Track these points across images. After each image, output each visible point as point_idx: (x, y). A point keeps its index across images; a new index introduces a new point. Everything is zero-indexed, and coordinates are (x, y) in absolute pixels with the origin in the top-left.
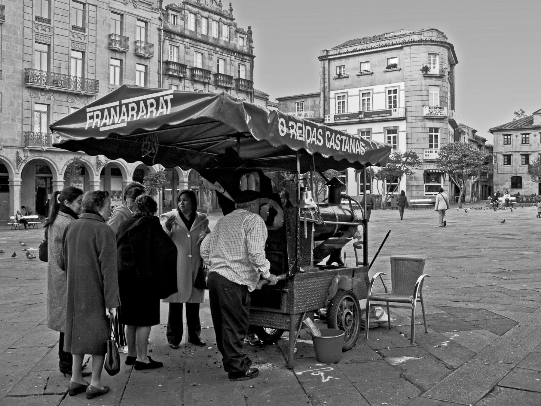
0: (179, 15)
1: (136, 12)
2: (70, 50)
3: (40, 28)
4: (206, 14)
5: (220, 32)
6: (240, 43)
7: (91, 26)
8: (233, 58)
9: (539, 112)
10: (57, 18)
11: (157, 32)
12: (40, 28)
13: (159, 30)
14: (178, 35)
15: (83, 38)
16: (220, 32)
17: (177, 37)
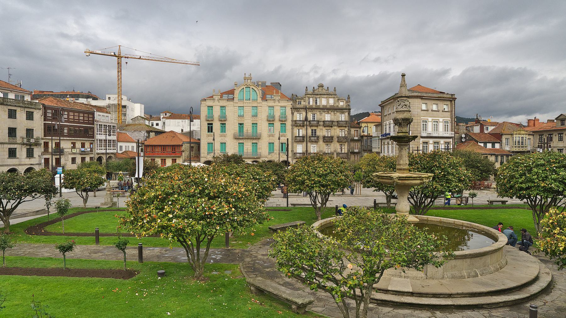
0: (302, 100)
1: (279, 104)
2: (251, 124)
3: (239, 119)
4: (318, 96)
5: (328, 102)
6: (342, 104)
7: (259, 114)
8: (336, 112)
9: (560, 118)
10: (246, 114)
11: (291, 110)
12: (239, 119)
13: (291, 109)
14: (302, 109)
15: (256, 119)
16: (328, 102)
17: (301, 110)
